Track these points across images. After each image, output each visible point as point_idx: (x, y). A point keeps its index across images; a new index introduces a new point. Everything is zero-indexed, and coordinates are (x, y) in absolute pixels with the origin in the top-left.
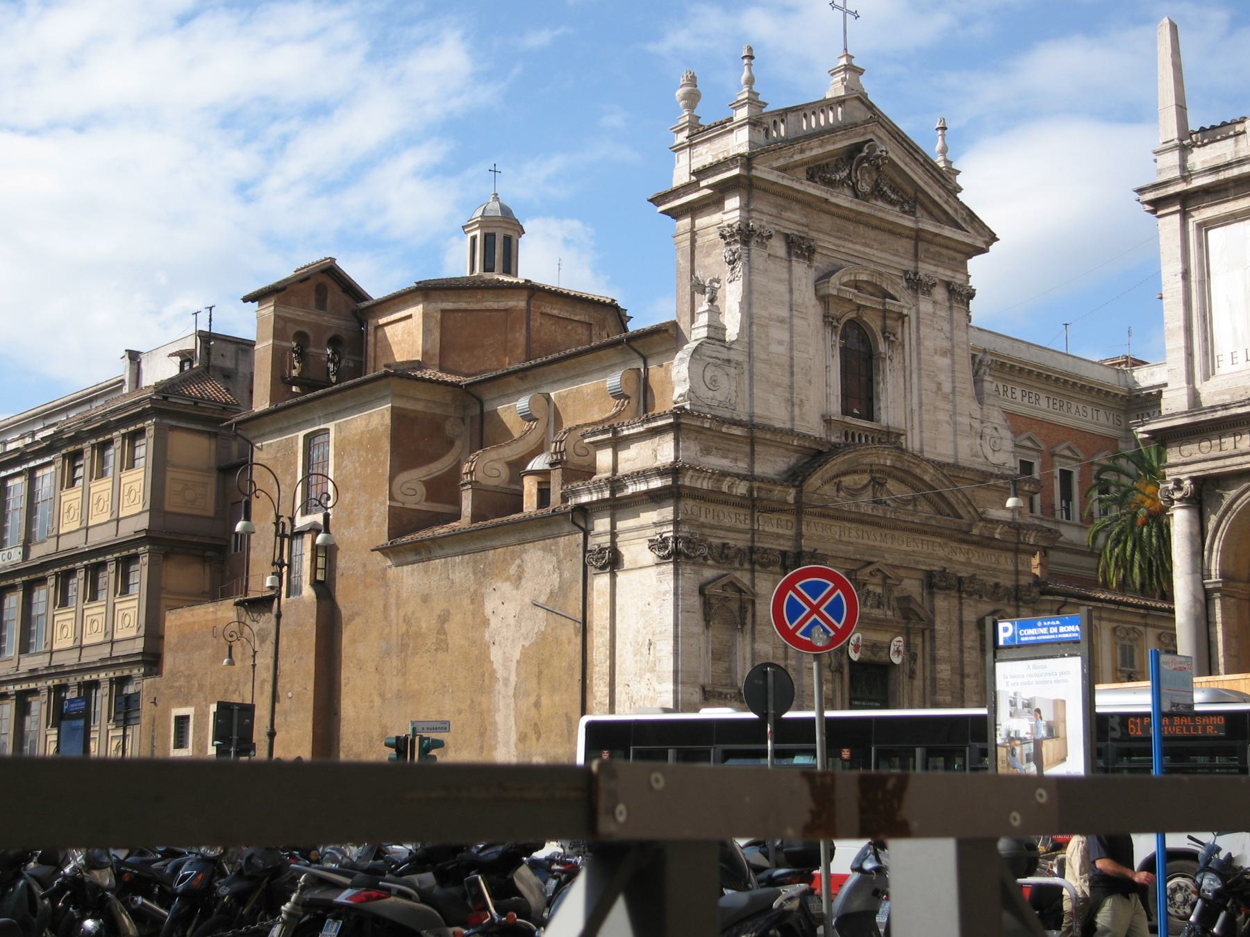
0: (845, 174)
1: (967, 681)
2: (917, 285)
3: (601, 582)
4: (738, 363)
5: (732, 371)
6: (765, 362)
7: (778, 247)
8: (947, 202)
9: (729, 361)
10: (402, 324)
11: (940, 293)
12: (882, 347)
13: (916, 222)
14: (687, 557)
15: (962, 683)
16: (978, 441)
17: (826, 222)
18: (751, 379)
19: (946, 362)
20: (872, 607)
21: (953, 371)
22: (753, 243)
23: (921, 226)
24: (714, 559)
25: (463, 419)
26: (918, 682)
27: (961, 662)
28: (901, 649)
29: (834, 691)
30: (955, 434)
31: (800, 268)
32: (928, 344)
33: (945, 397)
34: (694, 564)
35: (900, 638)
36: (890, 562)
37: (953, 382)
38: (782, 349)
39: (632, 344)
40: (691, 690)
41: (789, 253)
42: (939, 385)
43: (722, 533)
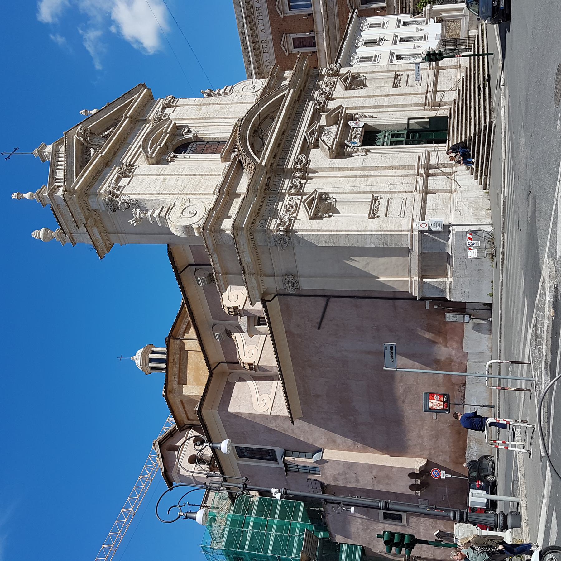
0: (92, 150)
3: (305, 285)
6: (185, 187)
7: (124, 181)
10: (185, 405)
11: (168, 111)
12: (190, 136)
18: (194, 194)
21: (209, 104)
22: (119, 192)
24: (292, 213)
25: (230, 373)
28: (355, 122)
35: (349, 122)
37: (215, 104)
38: (181, 179)
39: (180, 271)
41: (130, 176)
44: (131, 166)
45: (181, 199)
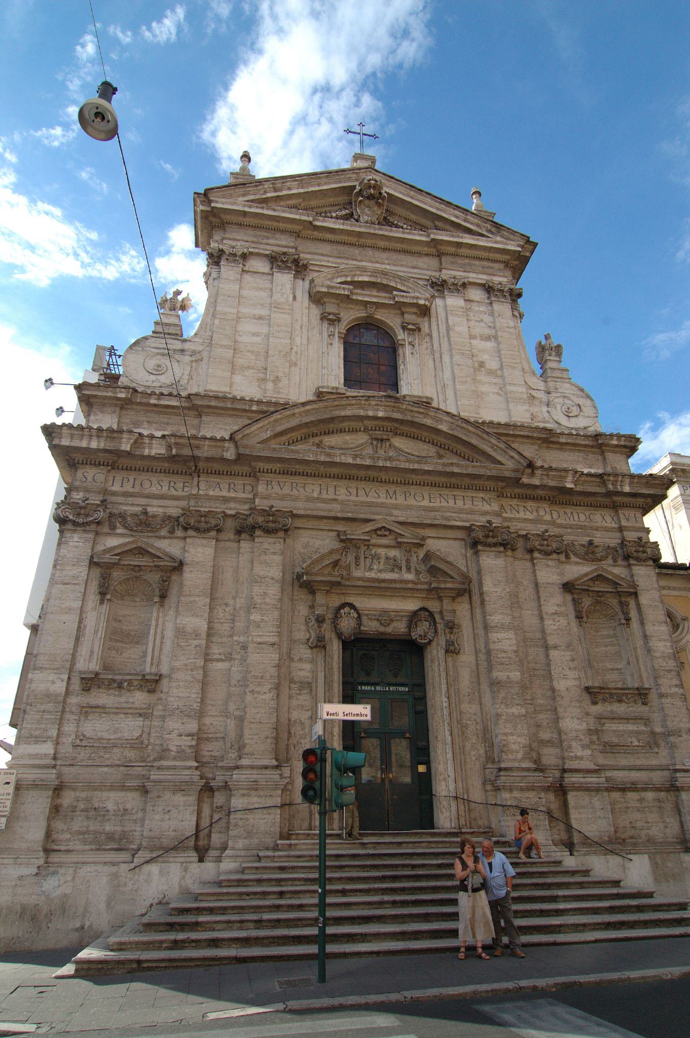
1: (553, 653)
2: (440, 286)
4: (194, 353)
5: (187, 359)
7: (261, 266)
8: (465, 221)
9: (182, 351)
13: (428, 236)
14: (75, 523)
15: (547, 656)
16: (545, 409)
17: (326, 248)
19: (490, 345)
20: (380, 571)
22: (222, 263)
23: (432, 236)
26: (467, 658)
27: (543, 631)
29: (314, 672)
30: (507, 402)
31: (284, 279)
32: (460, 326)
33: (491, 373)
34: (85, 531)
36: (401, 519)
40: (52, 677)
42: (482, 364)
43: (143, 501)
44: (299, 268)
45: (200, 348)
